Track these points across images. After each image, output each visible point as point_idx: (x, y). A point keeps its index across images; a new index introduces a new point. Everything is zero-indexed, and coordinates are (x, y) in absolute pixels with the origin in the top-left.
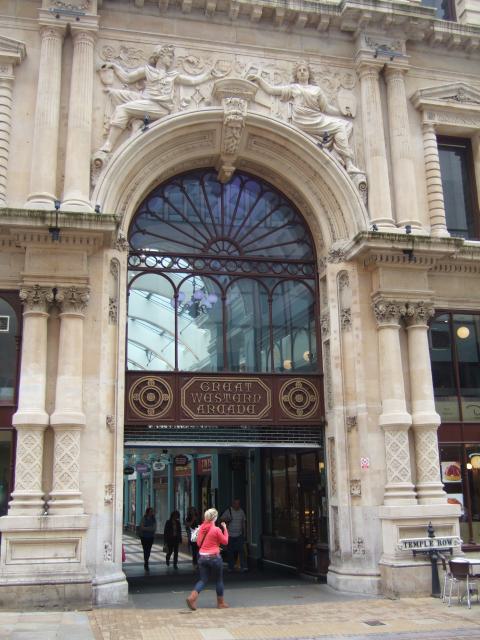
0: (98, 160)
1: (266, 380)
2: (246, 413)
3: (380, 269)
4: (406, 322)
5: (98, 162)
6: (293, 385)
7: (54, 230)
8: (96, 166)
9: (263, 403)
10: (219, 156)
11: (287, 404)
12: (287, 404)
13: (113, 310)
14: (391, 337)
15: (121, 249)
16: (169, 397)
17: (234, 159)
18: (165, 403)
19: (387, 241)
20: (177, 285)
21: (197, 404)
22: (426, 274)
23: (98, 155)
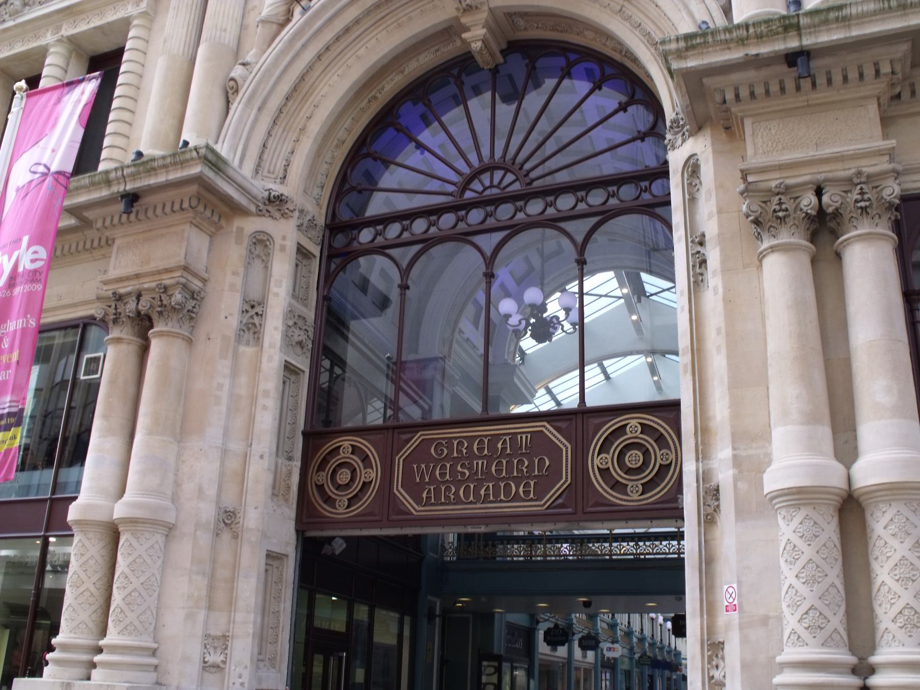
0: (232, 79)
1: (563, 425)
2: (517, 498)
3: (748, 123)
4: (823, 230)
5: (232, 83)
6: (622, 430)
7: (132, 199)
8: (230, 91)
9: (554, 474)
10: (457, 19)
11: (604, 472)
12: (604, 472)
13: (256, 320)
14: (780, 276)
15: (277, 215)
16: (373, 474)
17: (483, 15)
18: (366, 485)
19: (726, 44)
20: (404, 265)
21: (422, 485)
22: (872, 110)
23: (237, 72)
